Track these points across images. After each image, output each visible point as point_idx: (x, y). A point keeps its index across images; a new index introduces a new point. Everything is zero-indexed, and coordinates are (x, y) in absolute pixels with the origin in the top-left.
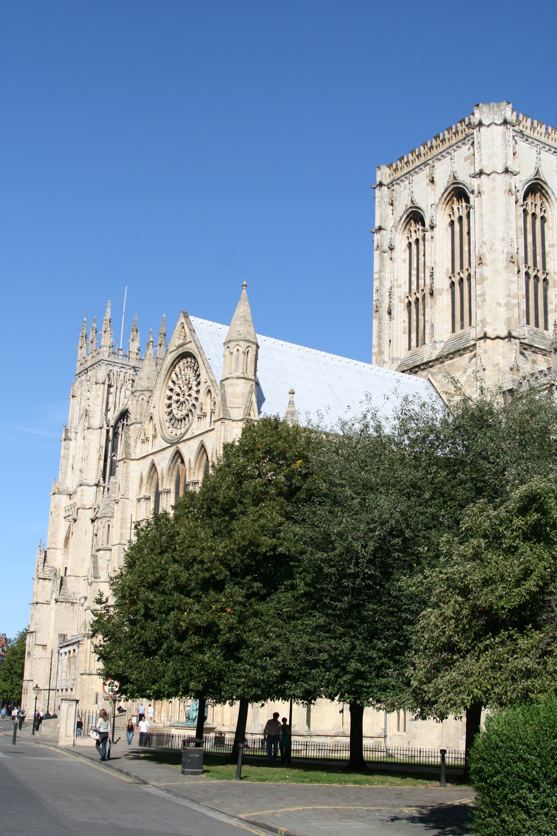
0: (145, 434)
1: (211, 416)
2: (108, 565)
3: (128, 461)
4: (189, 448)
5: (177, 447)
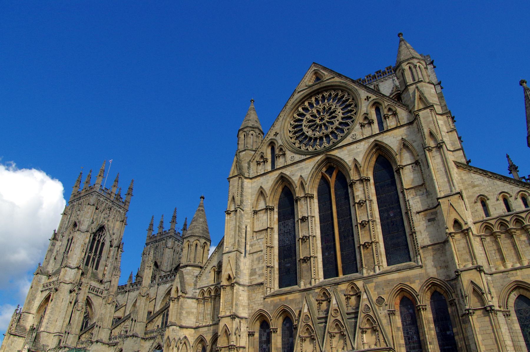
0: (262, 157)
1: (381, 124)
2: (196, 281)
3: (243, 178)
4: (349, 151)
5: (326, 155)
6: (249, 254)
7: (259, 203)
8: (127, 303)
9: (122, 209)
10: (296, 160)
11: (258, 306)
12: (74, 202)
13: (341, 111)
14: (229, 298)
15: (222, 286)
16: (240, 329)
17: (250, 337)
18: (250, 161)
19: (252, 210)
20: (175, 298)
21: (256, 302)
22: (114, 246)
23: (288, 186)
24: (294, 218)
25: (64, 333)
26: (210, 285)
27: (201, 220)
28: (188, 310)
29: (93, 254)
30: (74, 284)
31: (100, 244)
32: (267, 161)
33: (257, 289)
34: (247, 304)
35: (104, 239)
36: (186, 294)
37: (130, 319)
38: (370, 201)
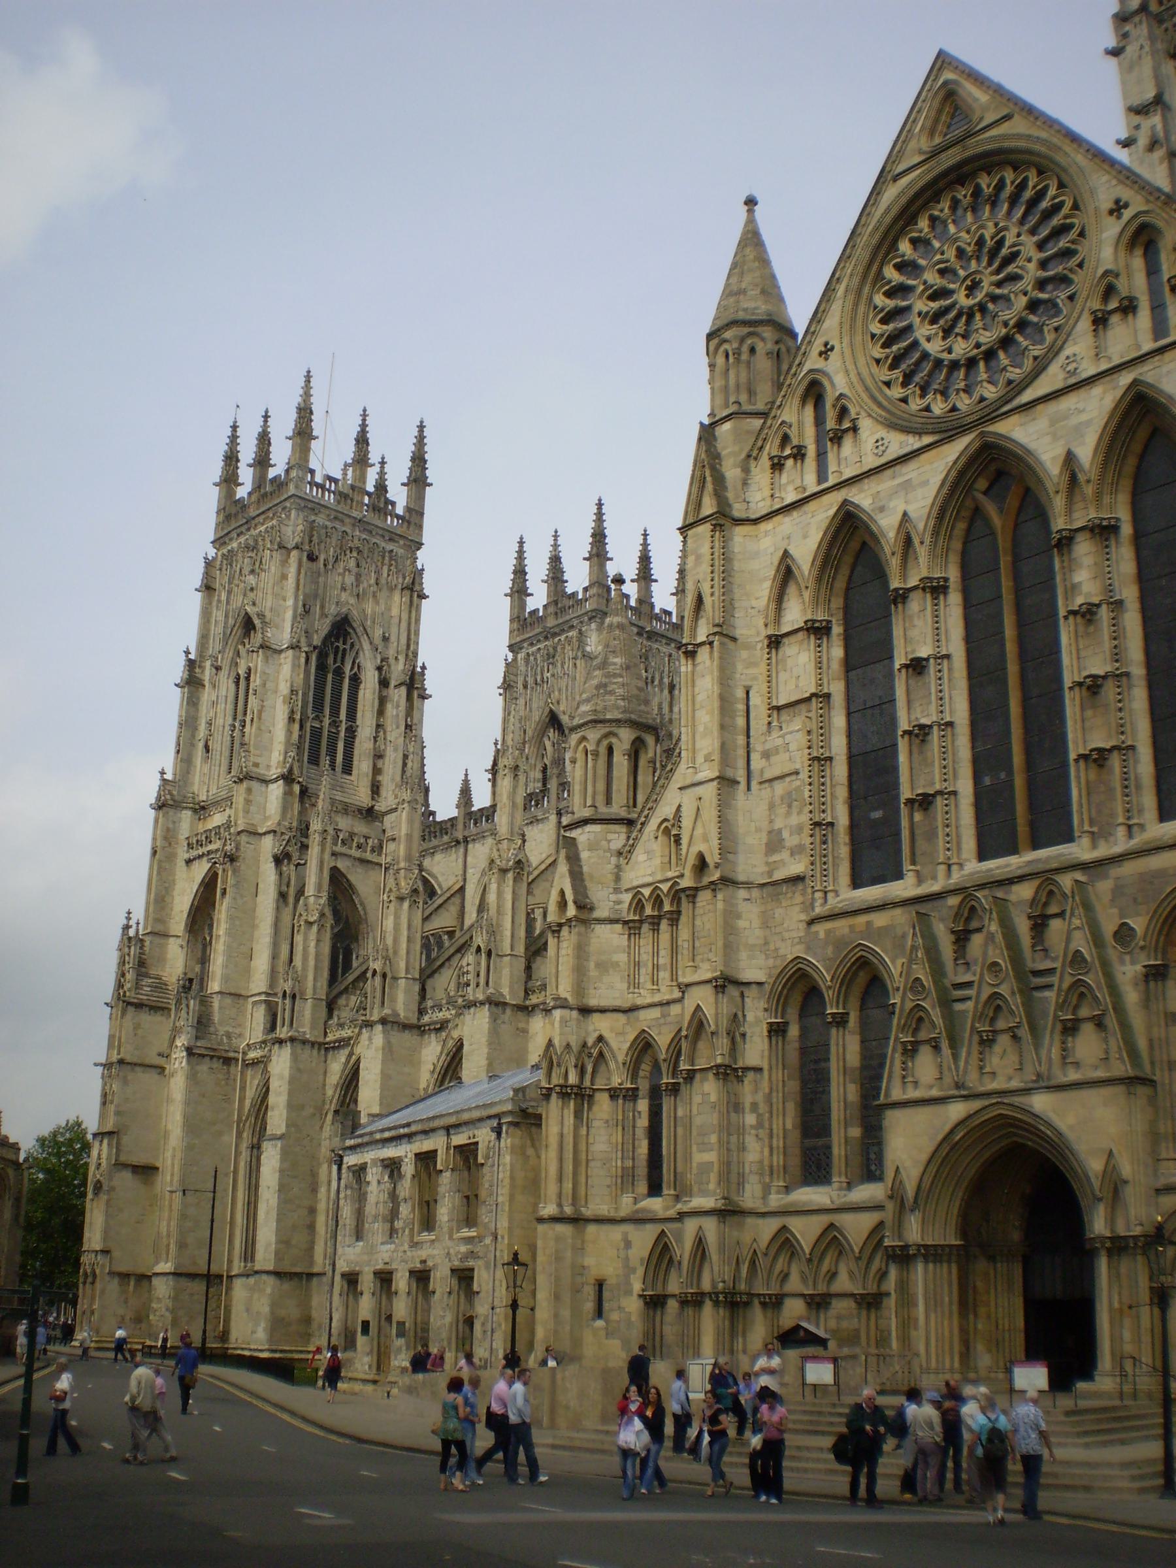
0: (785, 439)
2: (618, 867)
3: (728, 524)
4: (1053, 422)
6: (761, 783)
7: (784, 605)
8: (465, 880)
9: (402, 542)
10: (891, 455)
11: (792, 946)
12: (231, 540)
13: (1038, 256)
14: (708, 926)
15: (684, 890)
16: (744, 1016)
17: (774, 1039)
18: (749, 456)
19: (764, 632)
20: (560, 925)
21: (786, 935)
22: (393, 683)
23: (871, 544)
24: (891, 658)
25: (280, 995)
26: (659, 877)
27: (618, 660)
28: (604, 958)
29: (327, 721)
30: (283, 833)
31: (347, 681)
32: (803, 456)
33: (789, 895)
34: (762, 942)
35: (354, 662)
36: (592, 909)
37: (473, 949)
38: (1116, 602)
